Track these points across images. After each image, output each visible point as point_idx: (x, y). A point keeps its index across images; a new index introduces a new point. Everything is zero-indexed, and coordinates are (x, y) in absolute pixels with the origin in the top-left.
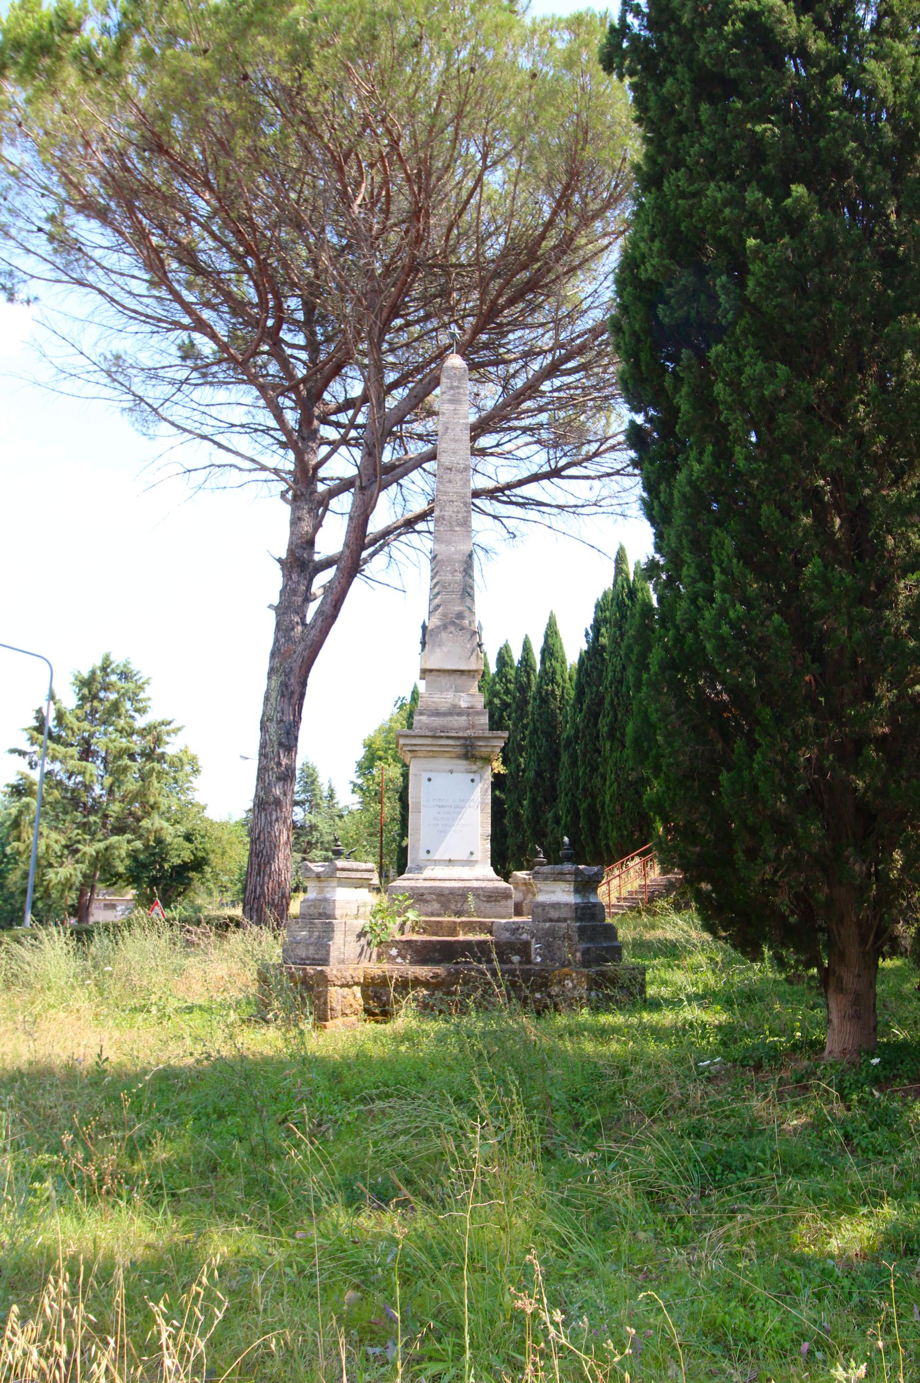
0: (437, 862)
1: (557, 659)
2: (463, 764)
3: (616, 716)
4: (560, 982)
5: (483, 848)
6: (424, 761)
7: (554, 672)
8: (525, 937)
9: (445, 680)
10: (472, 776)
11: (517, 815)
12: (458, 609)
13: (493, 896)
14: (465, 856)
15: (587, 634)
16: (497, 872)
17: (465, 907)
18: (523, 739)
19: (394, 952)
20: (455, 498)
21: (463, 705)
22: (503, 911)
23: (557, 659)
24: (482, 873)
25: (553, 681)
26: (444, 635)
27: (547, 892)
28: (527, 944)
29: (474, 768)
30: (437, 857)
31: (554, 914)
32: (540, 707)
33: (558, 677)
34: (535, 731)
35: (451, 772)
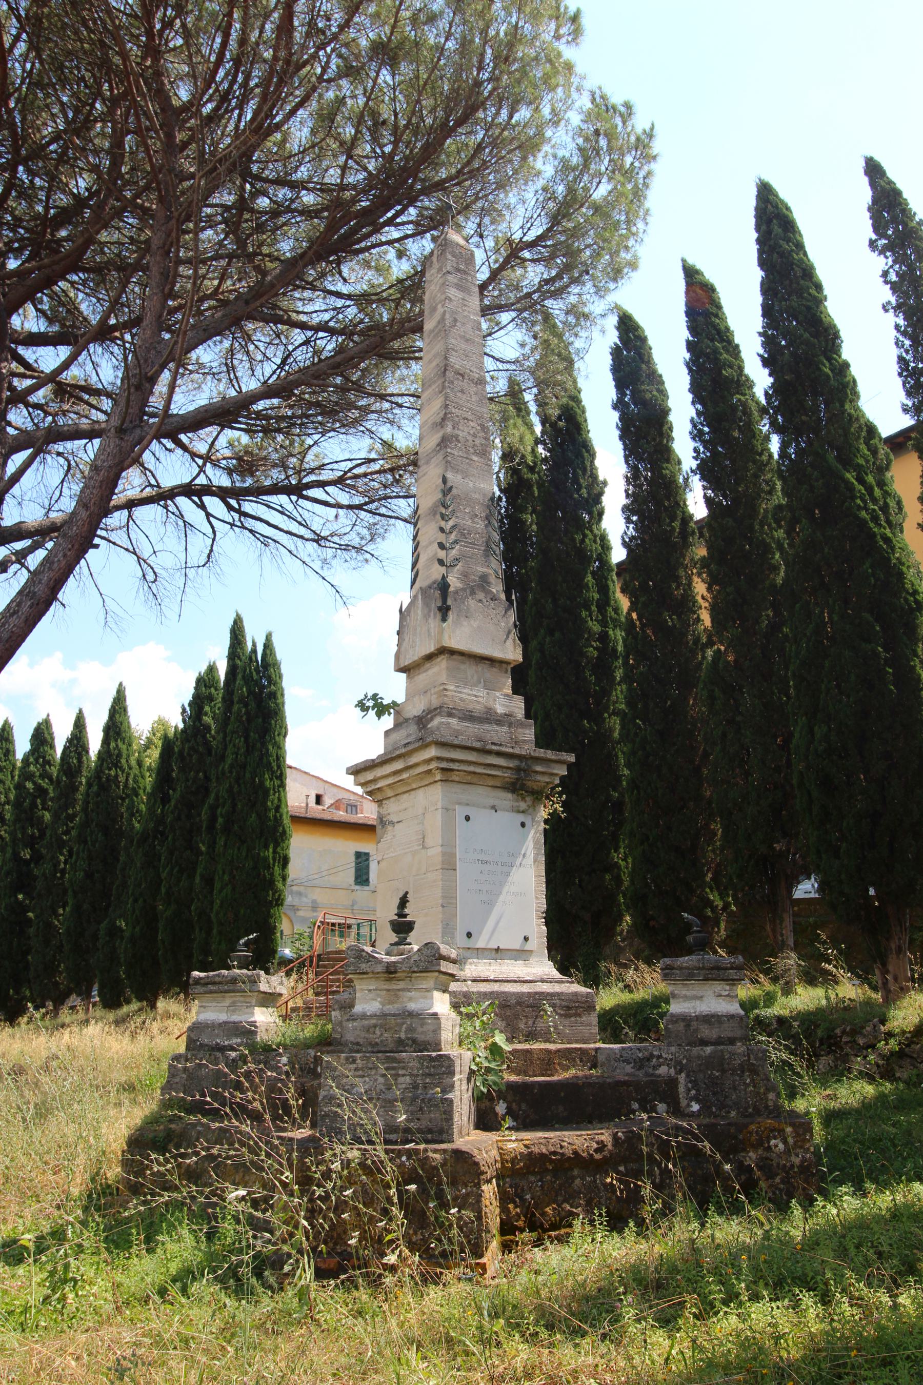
0: (480, 953)
1: (123, 740)
2: (506, 799)
3: (234, 805)
4: (761, 1143)
5: (538, 932)
6: (457, 788)
7: (119, 755)
8: (663, 1070)
9: (471, 670)
10: (521, 818)
11: (49, 925)
12: (481, 569)
13: (572, 1008)
14: (517, 944)
15: (184, 711)
16: (563, 969)
17: (540, 1025)
18: (67, 833)
19: (501, 1108)
20: (469, 415)
21: (500, 710)
22: (585, 1030)
23: (123, 740)
24: (538, 971)
25: (117, 765)
26: (472, 602)
27: (686, 998)
28: (672, 1083)
29: (523, 805)
30: (481, 944)
31: (706, 1032)
32: (98, 795)
33: (123, 761)
34: (85, 824)
35: (494, 808)
